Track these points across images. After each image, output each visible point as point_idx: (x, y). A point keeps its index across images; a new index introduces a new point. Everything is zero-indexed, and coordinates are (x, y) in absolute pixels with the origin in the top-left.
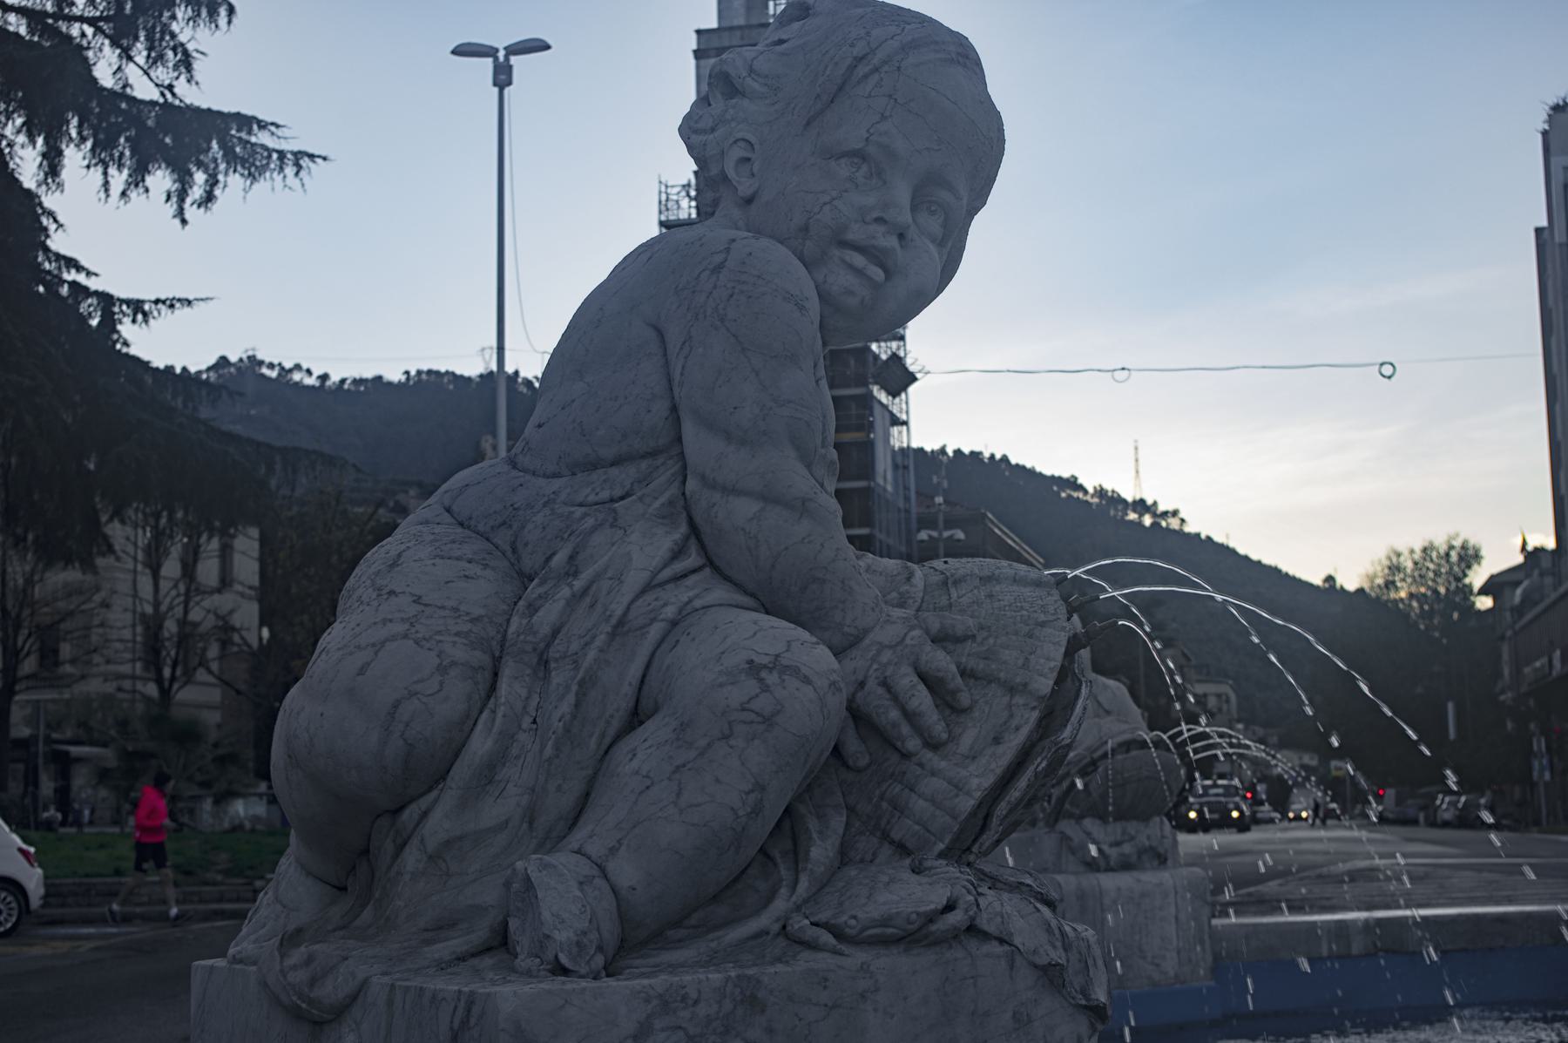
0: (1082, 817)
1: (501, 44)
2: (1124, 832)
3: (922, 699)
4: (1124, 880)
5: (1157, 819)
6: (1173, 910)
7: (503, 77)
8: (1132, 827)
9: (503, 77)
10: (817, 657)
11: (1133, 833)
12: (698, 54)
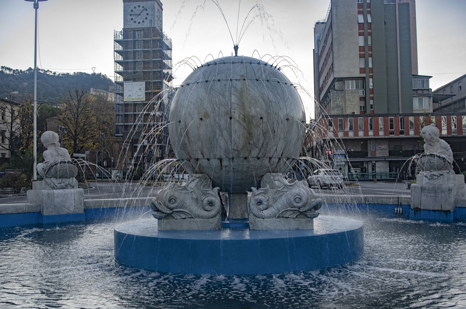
0: (51, 178)
2: (62, 181)
4: (61, 191)
5: (72, 178)
6: (73, 197)
8: (64, 180)
11: (64, 181)
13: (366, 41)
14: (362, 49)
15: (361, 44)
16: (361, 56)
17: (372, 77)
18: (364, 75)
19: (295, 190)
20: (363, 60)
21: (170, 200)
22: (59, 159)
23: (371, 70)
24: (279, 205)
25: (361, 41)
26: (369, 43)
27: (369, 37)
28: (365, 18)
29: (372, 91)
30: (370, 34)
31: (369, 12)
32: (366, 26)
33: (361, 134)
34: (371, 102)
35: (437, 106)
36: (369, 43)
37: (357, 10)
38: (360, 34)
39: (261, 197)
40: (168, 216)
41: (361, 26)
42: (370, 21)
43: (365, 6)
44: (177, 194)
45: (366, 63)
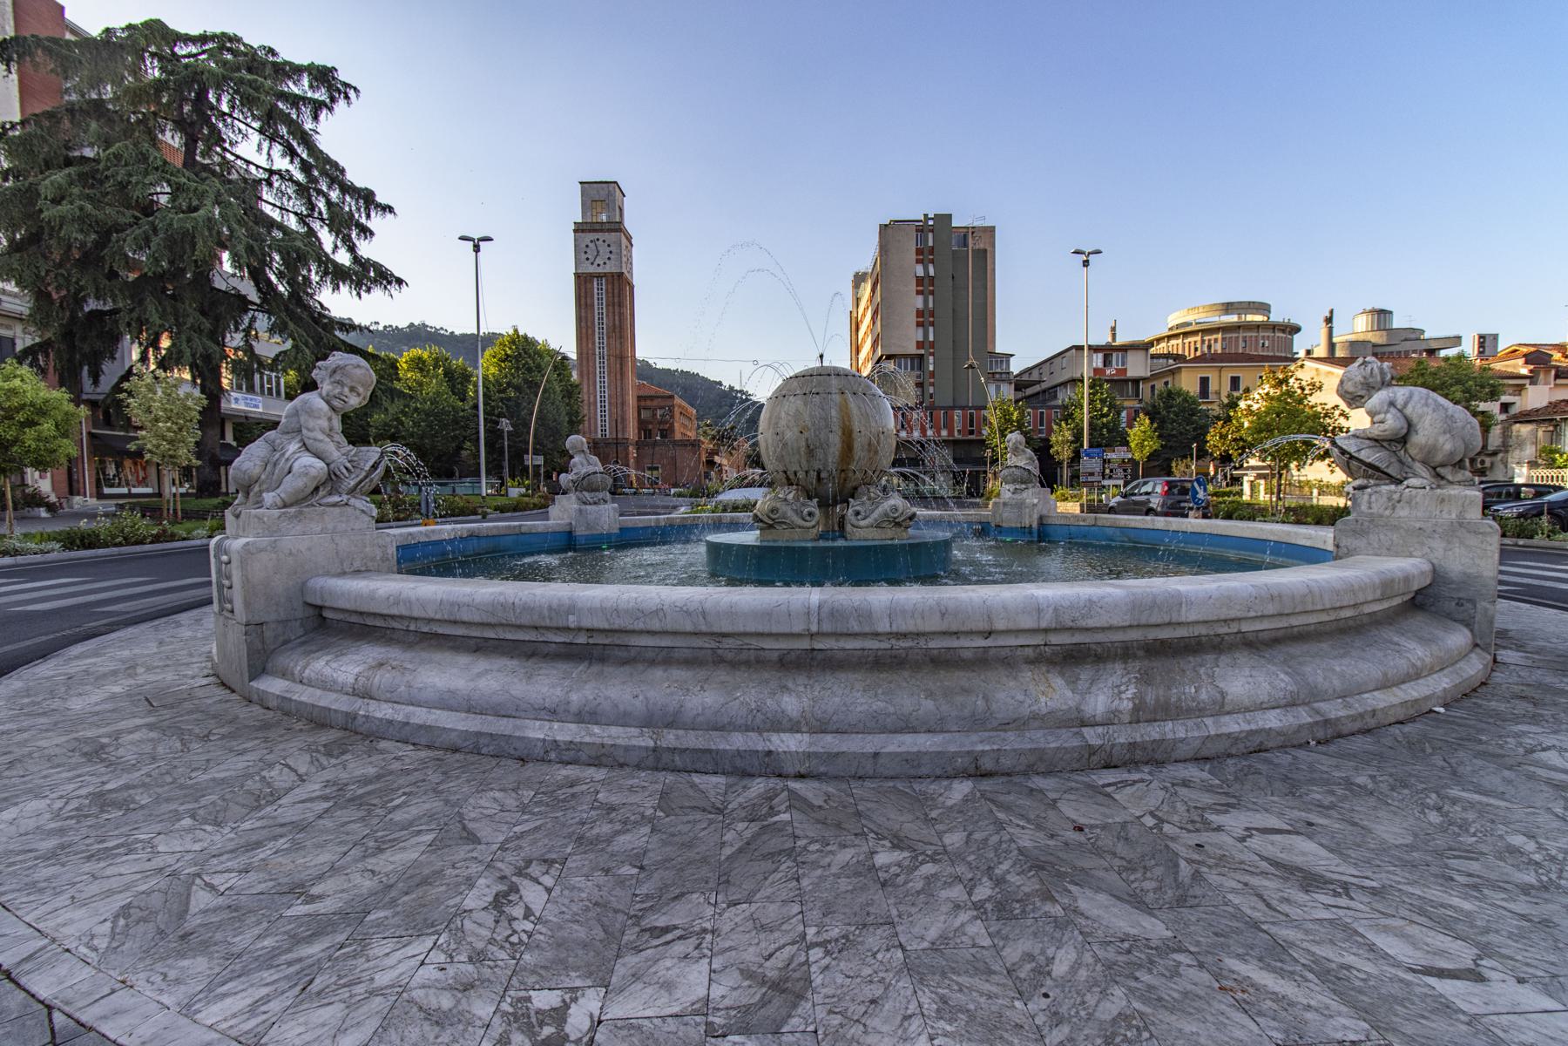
1: (476, 237)
3: (344, 471)
7: (477, 249)
9: (477, 249)
10: (320, 464)
12: (575, 231)
13: (926, 302)
14: (920, 313)
15: (920, 305)
16: (919, 324)
17: (932, 354)
18: (922, 352)
19: (892, 502)
20: (920, 331)
21: (772, 511)
22: (591, 469)
23: (932, 345)
24: (875, 515)
25: (919, 302)
26: (931, 305)
27: (931, 297)
28: (926, 270)
29: (932, 374)
30: (932, 293)
31: (932, 261)
32: (926, 281)
33: (916, 434)
34: (931, 390)
35: (1020, 395)
36: (931, 305)
37: (914, 257)
38: (918, 293)
39: (858, 508)
40: (771, 526)
41: (920, 281)
42: (932, 272)
43: (926, 252)
44: (778, 505)
45: (926, 335)
